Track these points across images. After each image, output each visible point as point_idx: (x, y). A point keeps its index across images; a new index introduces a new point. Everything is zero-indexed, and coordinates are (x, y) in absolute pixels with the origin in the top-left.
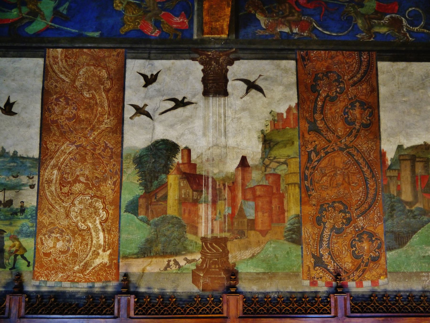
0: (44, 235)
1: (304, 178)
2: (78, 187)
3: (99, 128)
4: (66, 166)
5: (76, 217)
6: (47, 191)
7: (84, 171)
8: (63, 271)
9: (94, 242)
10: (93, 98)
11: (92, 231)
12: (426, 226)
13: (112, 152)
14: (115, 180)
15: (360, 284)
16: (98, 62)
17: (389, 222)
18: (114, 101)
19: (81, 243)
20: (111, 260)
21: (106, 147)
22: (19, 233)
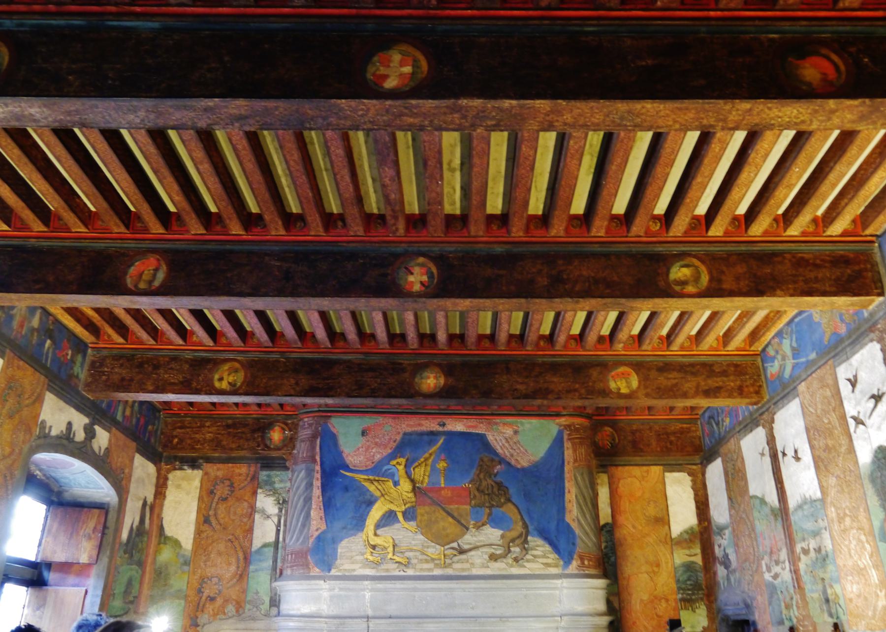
10: (830, 423)
21: (850, 471)
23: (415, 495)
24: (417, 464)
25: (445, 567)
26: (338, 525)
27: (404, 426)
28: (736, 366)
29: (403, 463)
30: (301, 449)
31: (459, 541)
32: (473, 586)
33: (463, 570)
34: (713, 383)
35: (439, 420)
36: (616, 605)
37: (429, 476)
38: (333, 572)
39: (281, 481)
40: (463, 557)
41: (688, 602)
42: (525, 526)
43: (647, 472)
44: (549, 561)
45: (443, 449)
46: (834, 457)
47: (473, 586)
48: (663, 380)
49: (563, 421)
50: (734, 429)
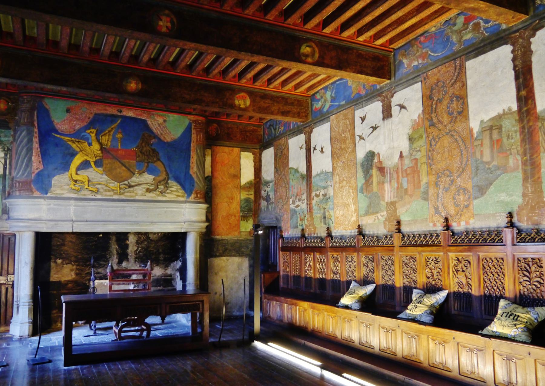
1: (429, 158)
2: (344, 183)
7: (345, 174)
10: (345, 137)
12: (499, 178)
15: (459, 224)
17: (475, 178)
21: (351, 160)
23: (102, 153)
24: (103, 134)
25: (120, 195)
26: (51, 167)
27: (95, 109)
28: (298, 101)
29: (95, 132)
30: (22, 117)
31: (129, 181)
32: (136, 205)
33: (131, 196)
34: (287, 108)
35: (118, 108)
36: (210, 217)
37: (111, 142)
38: (49, 195)
39: (6, 136)
40: (131, 189)
41: (245, 217)
42: (167, 174)
43: (232, 150)
44: (179, 194)
45: (120, 126)
46: (344, 153)
47: (136, 205)
48: (263, 103)
49: (192, 117)
50: (286, 133)
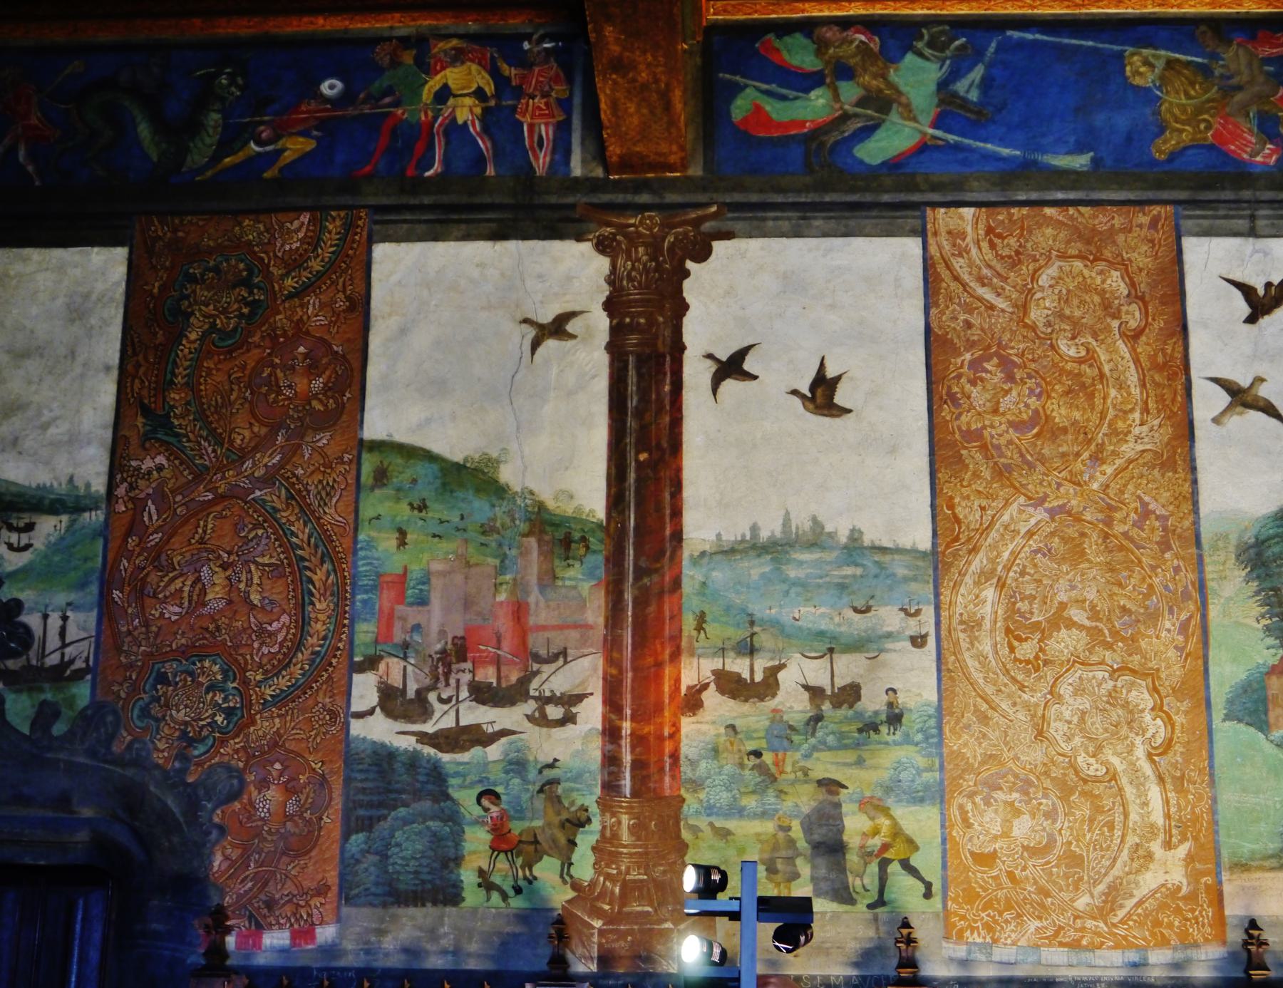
0: (971, 796)
2: (1065, 642)
3: (1115, 454)
4: (1023, 573)
5: (1069, 739)
6: (966, 655)
7: (1080, 588)
8: (1041, 911)
9: (1133, 817)
10: (1090, 358)
11: (1124, 781)
13: (1165, 529)
14: (1183, 617)
16: (1094, 247)
18: (1159, 368)
19: (1092, 820)
20: (1194, 876)
21: (1146, 513)
22: (890, 788)
